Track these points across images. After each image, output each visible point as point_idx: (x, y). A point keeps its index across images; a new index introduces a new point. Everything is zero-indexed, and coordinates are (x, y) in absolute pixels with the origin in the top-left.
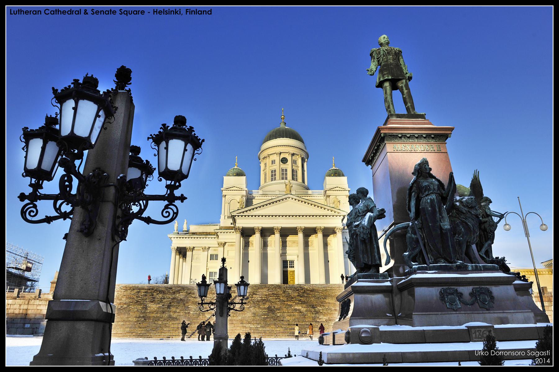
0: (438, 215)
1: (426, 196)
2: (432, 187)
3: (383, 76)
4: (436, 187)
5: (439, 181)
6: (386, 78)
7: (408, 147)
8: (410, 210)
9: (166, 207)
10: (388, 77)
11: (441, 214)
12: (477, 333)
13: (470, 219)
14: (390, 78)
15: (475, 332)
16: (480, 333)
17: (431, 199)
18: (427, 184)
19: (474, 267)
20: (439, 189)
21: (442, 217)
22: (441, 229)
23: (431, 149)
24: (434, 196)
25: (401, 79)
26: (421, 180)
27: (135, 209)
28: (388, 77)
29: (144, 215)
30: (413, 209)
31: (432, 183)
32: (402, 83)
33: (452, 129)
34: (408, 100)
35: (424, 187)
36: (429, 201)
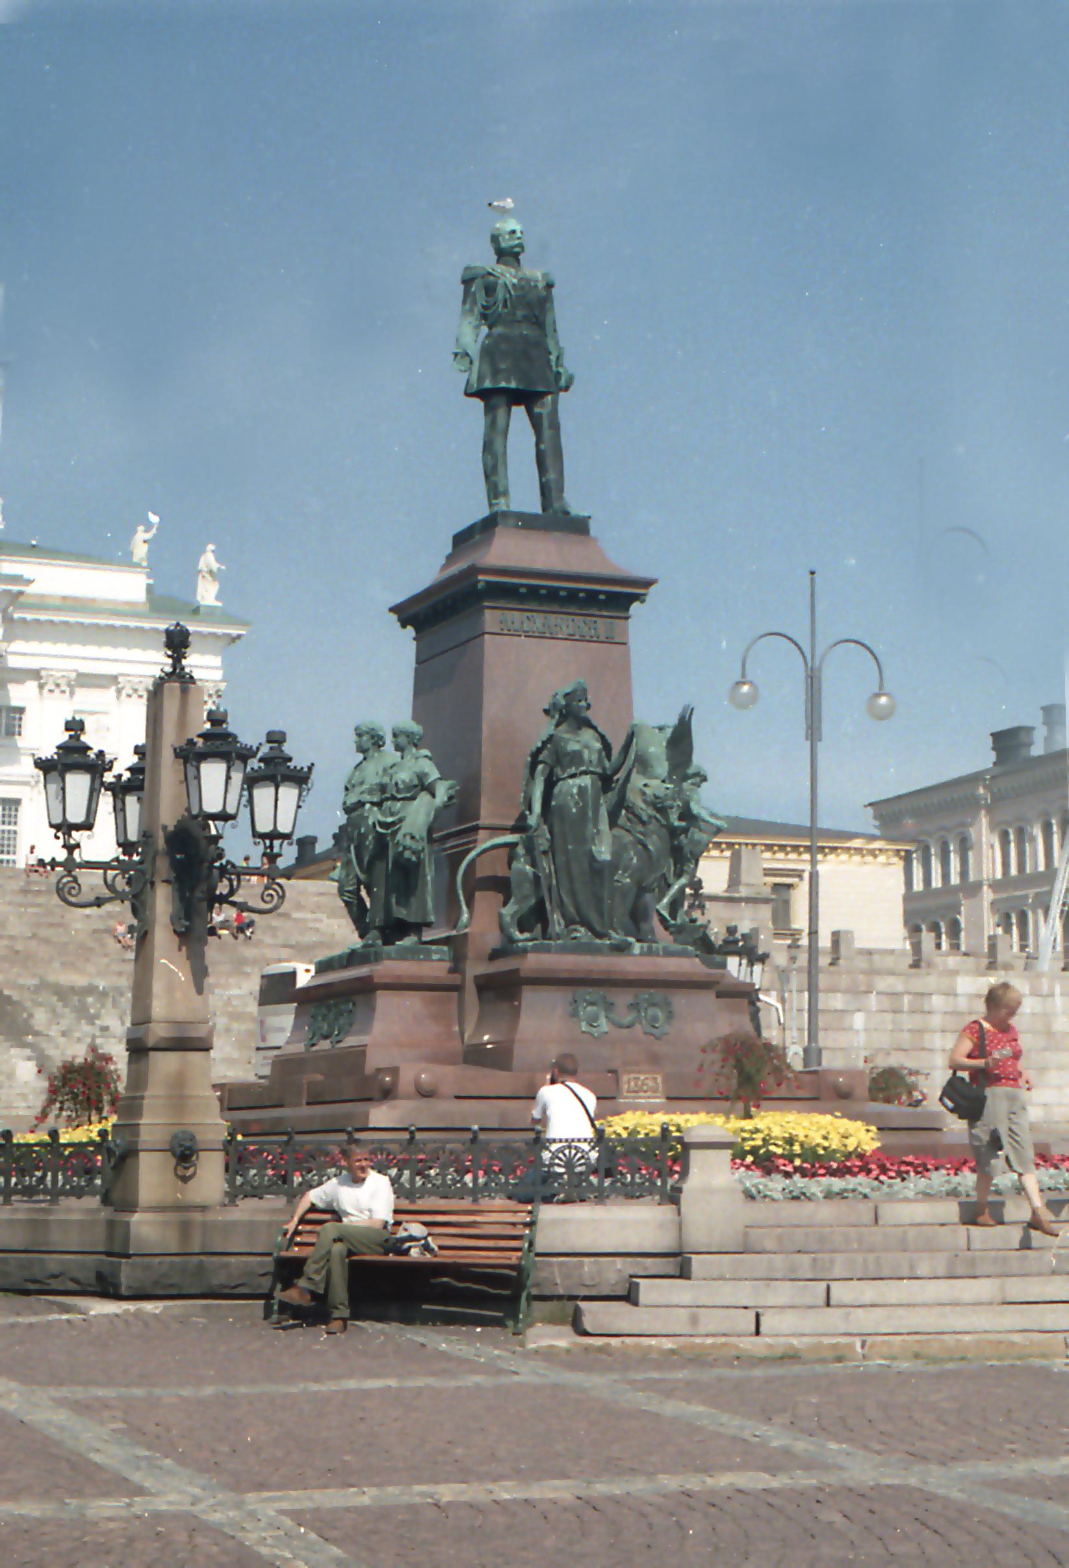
0: (590, 826)
1: (573, 776)
2: (586, 754)
3: (496, 373)
4: (595, 757)
5: (603, 738)
6: (503, 384)
7: (538, 621)
8: (530, 808)
9: (267, 888)
10: (508, 381)
11: (596, 825)
12: (632, 1084)
13: (654, 837)
14: (513, 385)
15: (629, 1082)
16: (636, 1085)
17: (580, 787)
18: (576, 747)
19: (645, 949)
20: (600, 760)
21: (599, 832)
22: (592, 858)
23: (593, 632)
24: (586, 781)
25: (543, 395)
26: (564, 732)
27: (222, 888)
28: (508, 381)
29: (234, 899)
30: (537, 807)
31: (587, 747)
32: (543, 406)
33: (648, 583)
34: (548, 459)
35: (568, 754)
36: (575, 791)
